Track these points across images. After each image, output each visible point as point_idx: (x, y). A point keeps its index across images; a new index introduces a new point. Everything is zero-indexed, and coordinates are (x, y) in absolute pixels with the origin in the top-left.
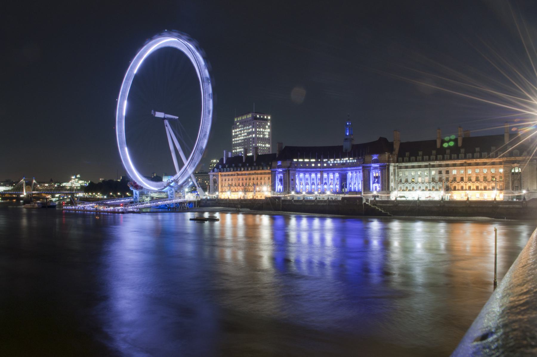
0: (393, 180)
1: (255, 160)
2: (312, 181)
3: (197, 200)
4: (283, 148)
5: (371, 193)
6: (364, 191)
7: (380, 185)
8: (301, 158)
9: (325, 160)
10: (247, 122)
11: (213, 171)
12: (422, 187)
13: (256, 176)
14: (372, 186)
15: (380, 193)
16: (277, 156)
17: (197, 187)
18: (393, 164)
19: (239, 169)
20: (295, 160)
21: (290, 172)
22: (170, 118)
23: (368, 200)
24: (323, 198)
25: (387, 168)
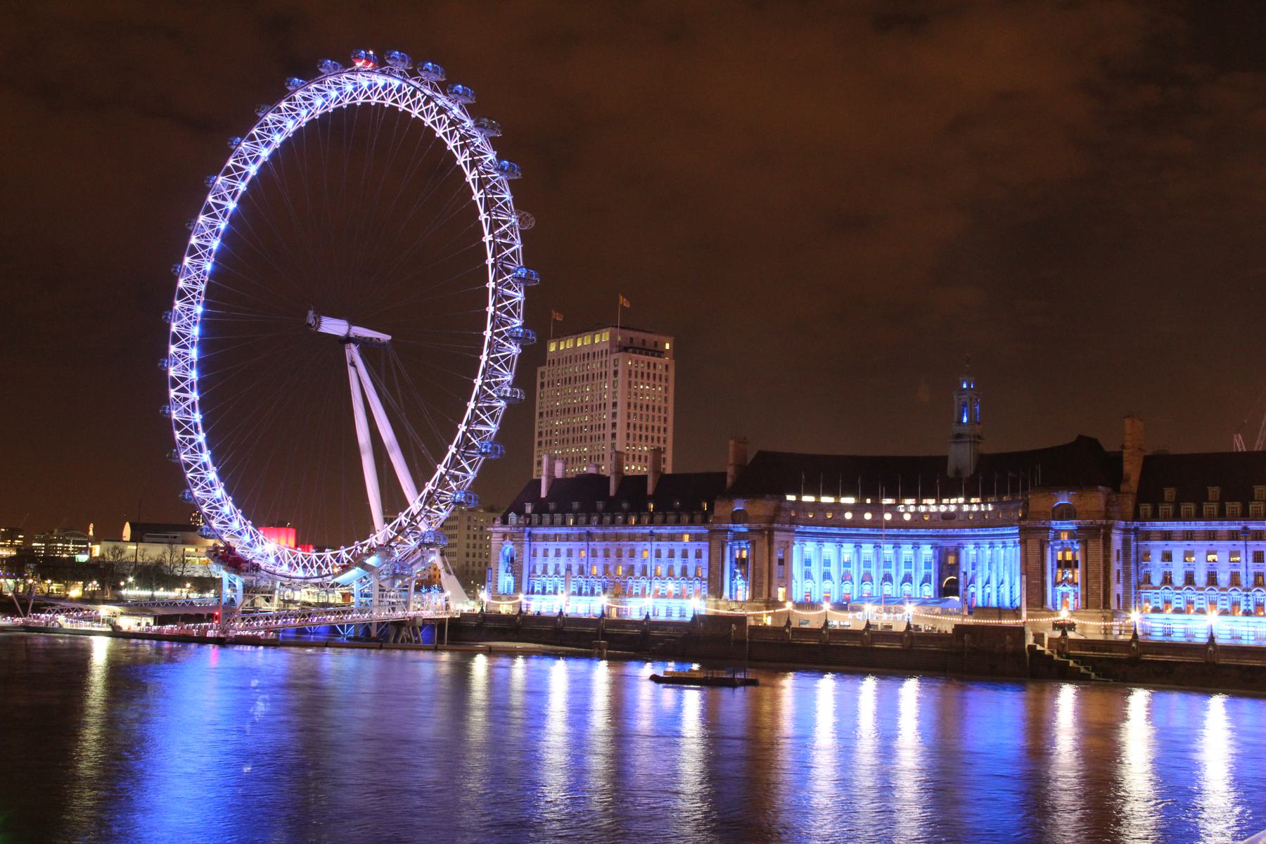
0: (1121, 574)
1: (650, 490)
2: (862, 569)
3: (448, 616)
4: (750, 457)
5: (1048, 616)
7: (1078, 589)
8: (808, 493)
11: (505, 522)
12: (1219, 603)
13: (655, 543)
14: (1053, 591)
15: (1079, 617)
16: (729, 481)
17: (443, 574)
18: (1123, 523)
20: (791, 498)
21: (775, 538)
22: (366, 338)
23: (1042, 635)
24: (886, 627)
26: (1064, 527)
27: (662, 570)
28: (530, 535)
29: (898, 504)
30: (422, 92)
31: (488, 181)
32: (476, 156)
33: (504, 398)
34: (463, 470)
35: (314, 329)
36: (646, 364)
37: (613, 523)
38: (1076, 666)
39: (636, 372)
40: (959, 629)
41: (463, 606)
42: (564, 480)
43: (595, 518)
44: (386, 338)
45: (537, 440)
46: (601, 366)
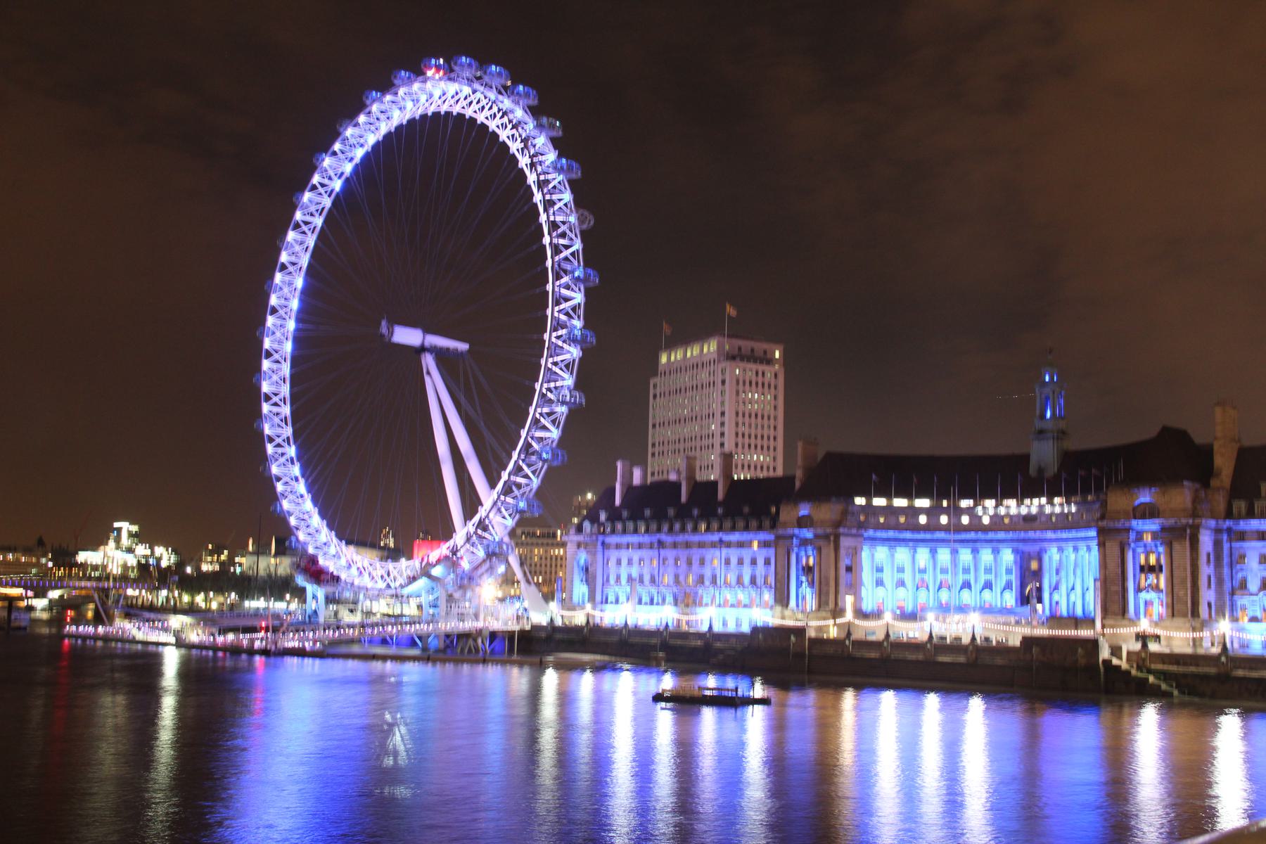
3: (516, 628)
4: (819, 459)
6: (1103, 618)
7: (1163, 596)
9: (965, 503)
10: (700, 366)
11: (579, 529)
13: (724, 551)
15: (1166, 628)
16: (798, 484)
18: (1212, 523)
19: (665, 527)
20: (860, 501)
23: (1120, 648)
25: (1188, 538)
26: (1146, 527)
27: (732, 578)
29: (976, 505)
31: (547, 182)
33: (563, 403)
34: (526, 476)
36: (754, 373)
37: (683, 530)
38: (1156, 682)
40: (1028, 641)
41: (540, 617)
42: (644, 488)
43: (689, 526)
44: (463, 346)
45: (650, 450)
46: (709, 374)
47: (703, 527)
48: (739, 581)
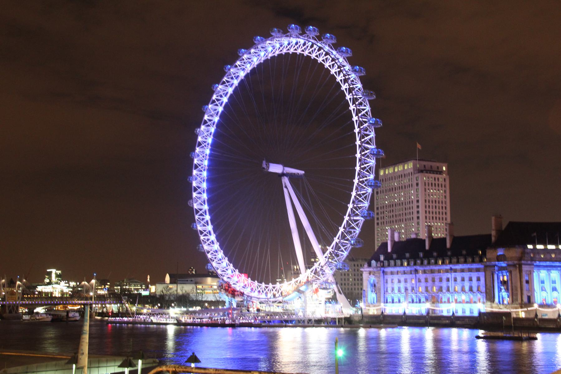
1: (448, 245)
8: (540, 243)
11: (370, 265)
13: (453, 274)
16: (493, 239)
19: (419, 262)
20: (530, 247)
21: (523, 269)
27: (458, 288)
28: (383, 272)
30: (316, 45)
31: (353, 89)
32: (347, 76)
34: (348, 240)
35: (266, 170)
36: (433, 179)
37: (429, 263)
39: (428, 184)
41: (349, 311)
42: (400, 242)
44: (301, 172)
46: (409, 181)
47: (448, 261)
48: (463, 290)
